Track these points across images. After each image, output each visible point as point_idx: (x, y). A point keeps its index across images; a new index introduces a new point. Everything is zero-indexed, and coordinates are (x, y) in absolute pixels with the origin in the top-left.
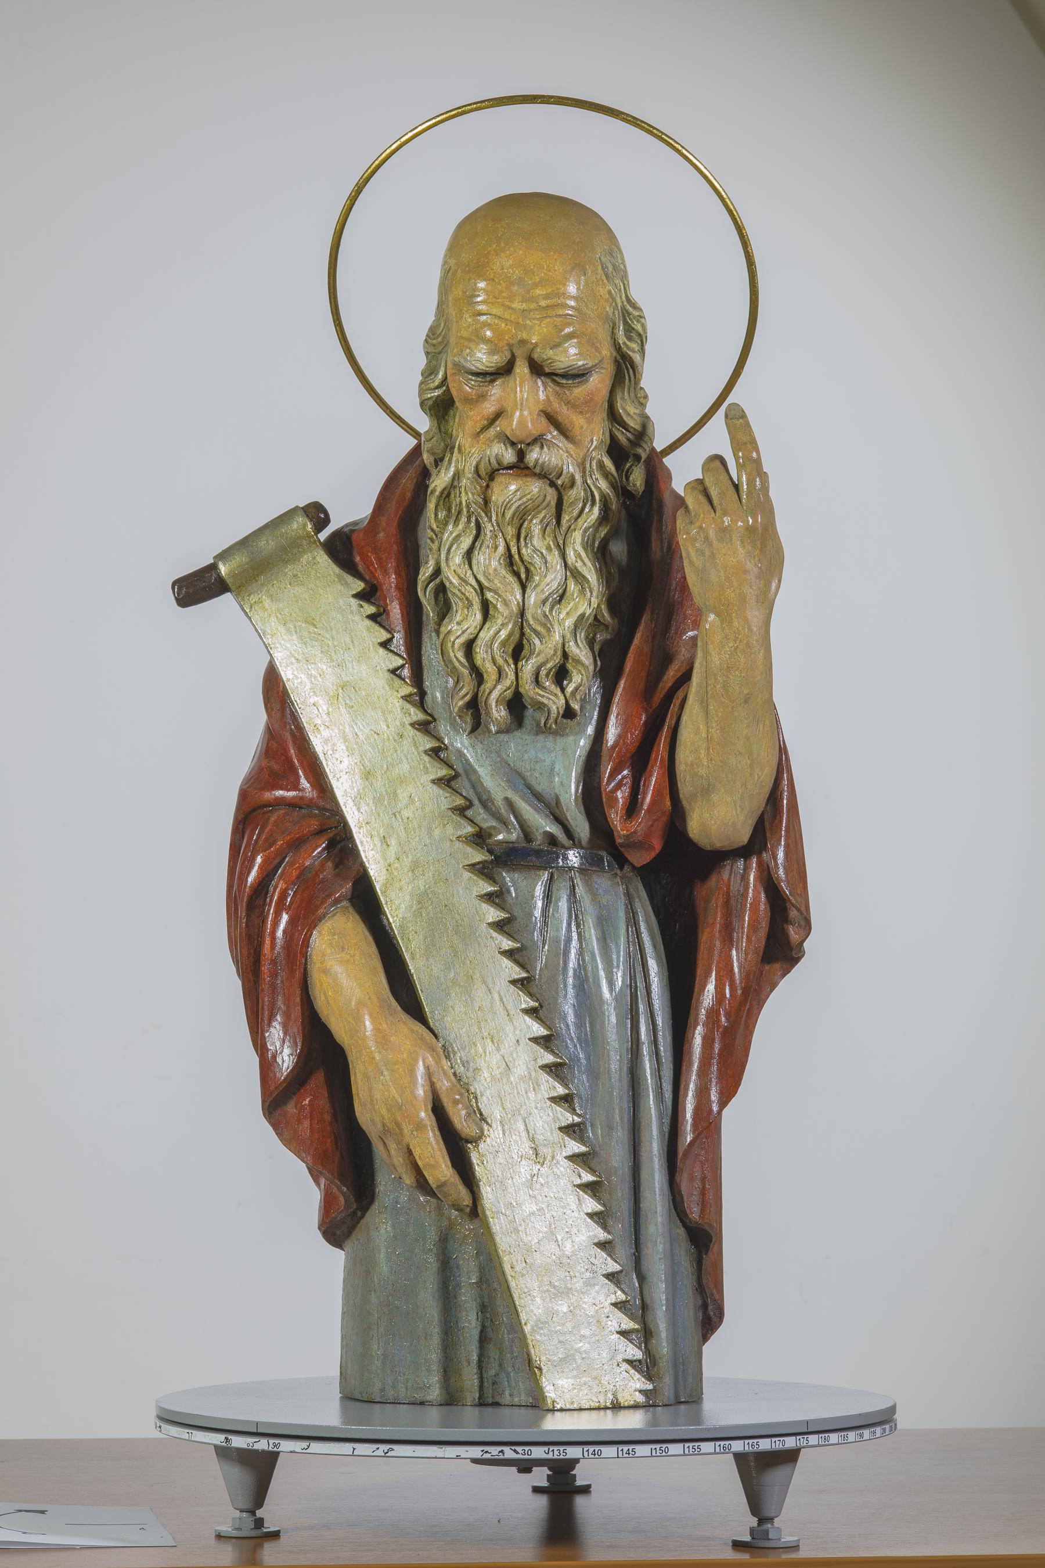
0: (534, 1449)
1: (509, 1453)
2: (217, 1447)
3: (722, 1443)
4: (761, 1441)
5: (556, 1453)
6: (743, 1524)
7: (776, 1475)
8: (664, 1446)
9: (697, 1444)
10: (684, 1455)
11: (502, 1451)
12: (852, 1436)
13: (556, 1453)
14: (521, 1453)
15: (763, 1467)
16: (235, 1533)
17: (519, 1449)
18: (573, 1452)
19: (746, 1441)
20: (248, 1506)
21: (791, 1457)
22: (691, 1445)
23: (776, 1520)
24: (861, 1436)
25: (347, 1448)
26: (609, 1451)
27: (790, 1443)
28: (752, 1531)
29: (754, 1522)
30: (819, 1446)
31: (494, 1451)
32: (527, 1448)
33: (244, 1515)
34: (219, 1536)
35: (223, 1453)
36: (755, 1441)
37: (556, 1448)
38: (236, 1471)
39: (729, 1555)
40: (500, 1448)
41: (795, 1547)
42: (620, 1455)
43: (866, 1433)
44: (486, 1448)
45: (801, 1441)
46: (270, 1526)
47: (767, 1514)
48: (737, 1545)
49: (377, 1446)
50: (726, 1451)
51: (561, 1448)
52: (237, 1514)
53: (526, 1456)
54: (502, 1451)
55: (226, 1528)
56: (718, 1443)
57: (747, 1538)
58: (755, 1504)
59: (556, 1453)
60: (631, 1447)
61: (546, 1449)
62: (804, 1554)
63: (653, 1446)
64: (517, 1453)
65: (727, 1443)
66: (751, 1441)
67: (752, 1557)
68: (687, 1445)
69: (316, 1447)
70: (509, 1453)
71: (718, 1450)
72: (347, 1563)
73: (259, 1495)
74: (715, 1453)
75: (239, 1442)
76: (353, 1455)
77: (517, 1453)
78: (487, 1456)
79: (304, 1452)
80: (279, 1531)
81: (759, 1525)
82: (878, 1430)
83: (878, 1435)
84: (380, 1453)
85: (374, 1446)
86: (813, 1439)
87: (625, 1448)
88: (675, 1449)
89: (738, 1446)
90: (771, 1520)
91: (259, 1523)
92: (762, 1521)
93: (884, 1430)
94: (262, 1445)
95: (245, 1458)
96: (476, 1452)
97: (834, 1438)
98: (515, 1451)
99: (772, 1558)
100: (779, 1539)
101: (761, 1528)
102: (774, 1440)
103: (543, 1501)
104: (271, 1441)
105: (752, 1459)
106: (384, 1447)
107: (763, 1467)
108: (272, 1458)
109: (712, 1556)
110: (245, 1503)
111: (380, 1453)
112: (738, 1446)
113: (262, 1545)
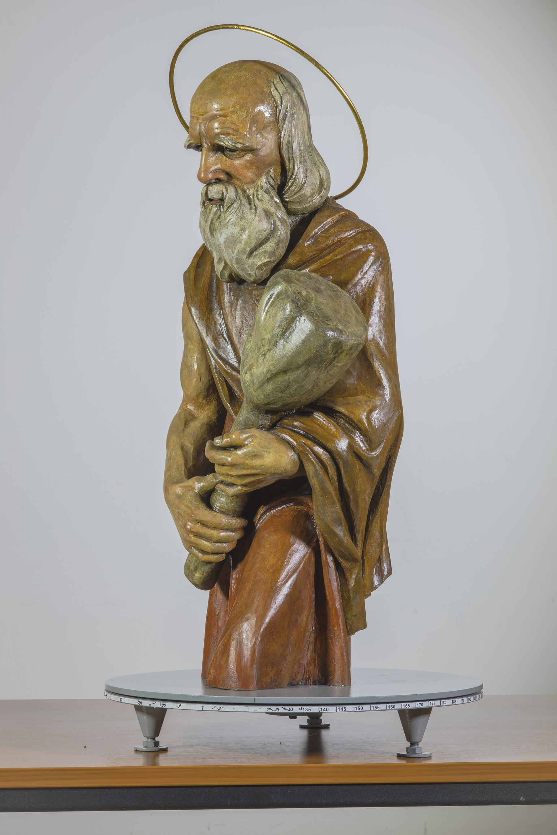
0: (294, 707)
1: (281, 710)
3: (390, 705)
4: (410, 703)
5: (305, 709)
6: (403, 745)
7: (420, 720)
8: (360, 706)
9: (377, 705)
10: (371, 711)
11: (278, 709)
12: (458, 701)
13: (305, 709)
14: (287, 709)
15: (412, 717)
17: (286, 707)
18: (314, 709)
19: (403, 704)
21: (427, 711)
22: (374, 705)
25: (199, 707)
26: (332, 709)
28: (407, 749)
30: (440, 706)
31: (274, 708)
32: (290, 707)
36: (408, 704)
37: (305, 707)
39: (395, 761)
40: (276, 707)
41: (429, 757)
42: (338, 711)
44: (269, 707)
45: (431, 704)
48: (400, 756)
50: (393, 709)
51: (308, 707)
53: (290, 711)
54: (278, 709)
56: (388, 705)
57: (405, 753)
58: (409, 737)
59: (305, 709)
60: (343, 707)
61: (300, 707)
62: (433, 761)
63: (355, 706)
64: (286, 709)
65: (393, 704)
66: (405, 704)
67: (407, 762)
68: (372, 706)
70: (281, 710)
71: (388, 708)
72: (199, 764)
75: (145, 703)
76: (202, 710)
77: (286, 709)
78: (270, 711)
79: (178, 709)
81: (411, 746)
83: (472, 700)
84: (216, 709)
85: (214, 706)
86: (438, 703)
87: (341, 707)
88: (366, 708)
89: (398, 706)
92: (412, 744)
93: (476, 698)
94: (157, 705)
95: (149, 711)
96: (264, 709)
97: (448, 702)
98: (284, 708)
99: (417, 763)
104: (162, 703)
105: (407, 712)
106: (218, 706)
107: (412, 717)
108: (163, 712)
109: (385, 762)
111: (216, 709)
112: (398, 706)
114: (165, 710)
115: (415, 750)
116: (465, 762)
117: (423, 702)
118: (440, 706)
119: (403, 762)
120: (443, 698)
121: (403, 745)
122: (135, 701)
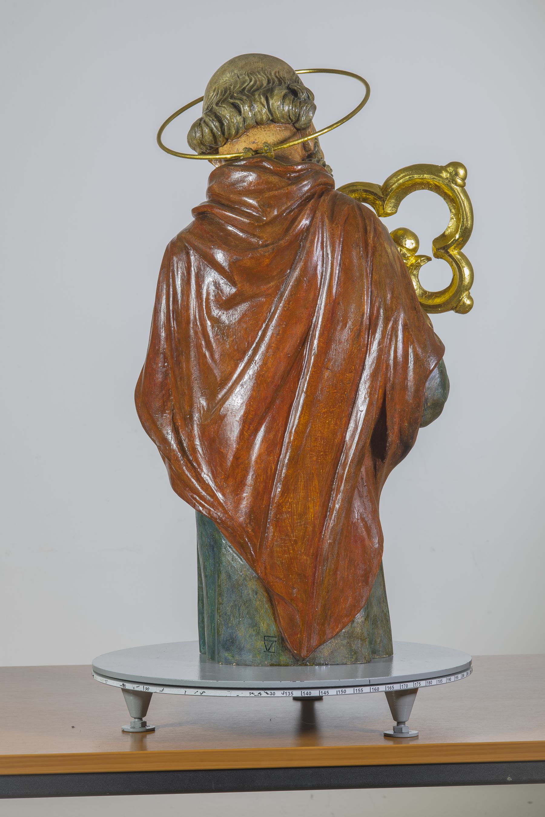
2: (122, 689)
7: (407, 700)
12: (444, 680)
16: (132, 730)
20: (138, 716)
21: (414, 691)
23: (406, 723)
24: (450, 680)
27: (411, 686)
28: (394, 728)
29: (395, 723)
30: (426, 686)
33: (137, 720)
34: (124, 731)
35: (125, 691)
38: (131, 698)
41: (416, 737)
43: (453, 678)
46: (150, 726)
47: (402, 720)
48: (387, 736)
49: (197, 690)
52: (133, 720)
55: (127, 727)
57: (391, 732)
58: (395, 716)
69: (167, 690)
73: (144, 711)
74: (370, 692)
80: (154, 728)
82: (460, 676)
86: (423, 683)
90: (404, 723)
91: (144, 724)
92: (399, 723)
97: (434, 682)
100: (408, 733)
101: (399, 727)
102: (401, 684)
103: (298, 705)
110: (136, 713)
113: (145, 737)
114: (151, 694)
115: (402, 729)
116: (451, 742)
117: (408, 684)
118: (426, 686)
119: (390, 744)
120: (428, 678)
121: (388, 725)
122: (119, 684)
